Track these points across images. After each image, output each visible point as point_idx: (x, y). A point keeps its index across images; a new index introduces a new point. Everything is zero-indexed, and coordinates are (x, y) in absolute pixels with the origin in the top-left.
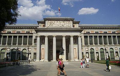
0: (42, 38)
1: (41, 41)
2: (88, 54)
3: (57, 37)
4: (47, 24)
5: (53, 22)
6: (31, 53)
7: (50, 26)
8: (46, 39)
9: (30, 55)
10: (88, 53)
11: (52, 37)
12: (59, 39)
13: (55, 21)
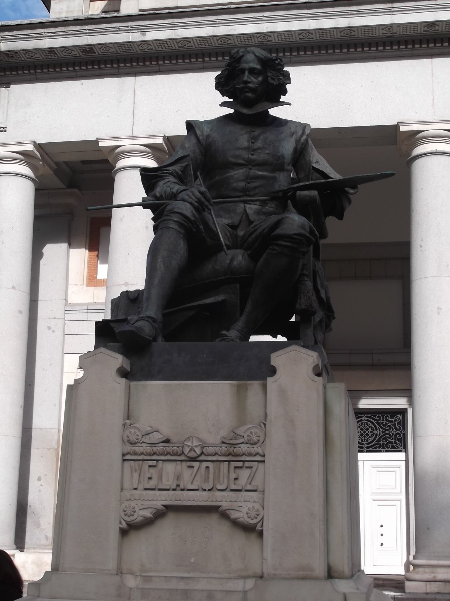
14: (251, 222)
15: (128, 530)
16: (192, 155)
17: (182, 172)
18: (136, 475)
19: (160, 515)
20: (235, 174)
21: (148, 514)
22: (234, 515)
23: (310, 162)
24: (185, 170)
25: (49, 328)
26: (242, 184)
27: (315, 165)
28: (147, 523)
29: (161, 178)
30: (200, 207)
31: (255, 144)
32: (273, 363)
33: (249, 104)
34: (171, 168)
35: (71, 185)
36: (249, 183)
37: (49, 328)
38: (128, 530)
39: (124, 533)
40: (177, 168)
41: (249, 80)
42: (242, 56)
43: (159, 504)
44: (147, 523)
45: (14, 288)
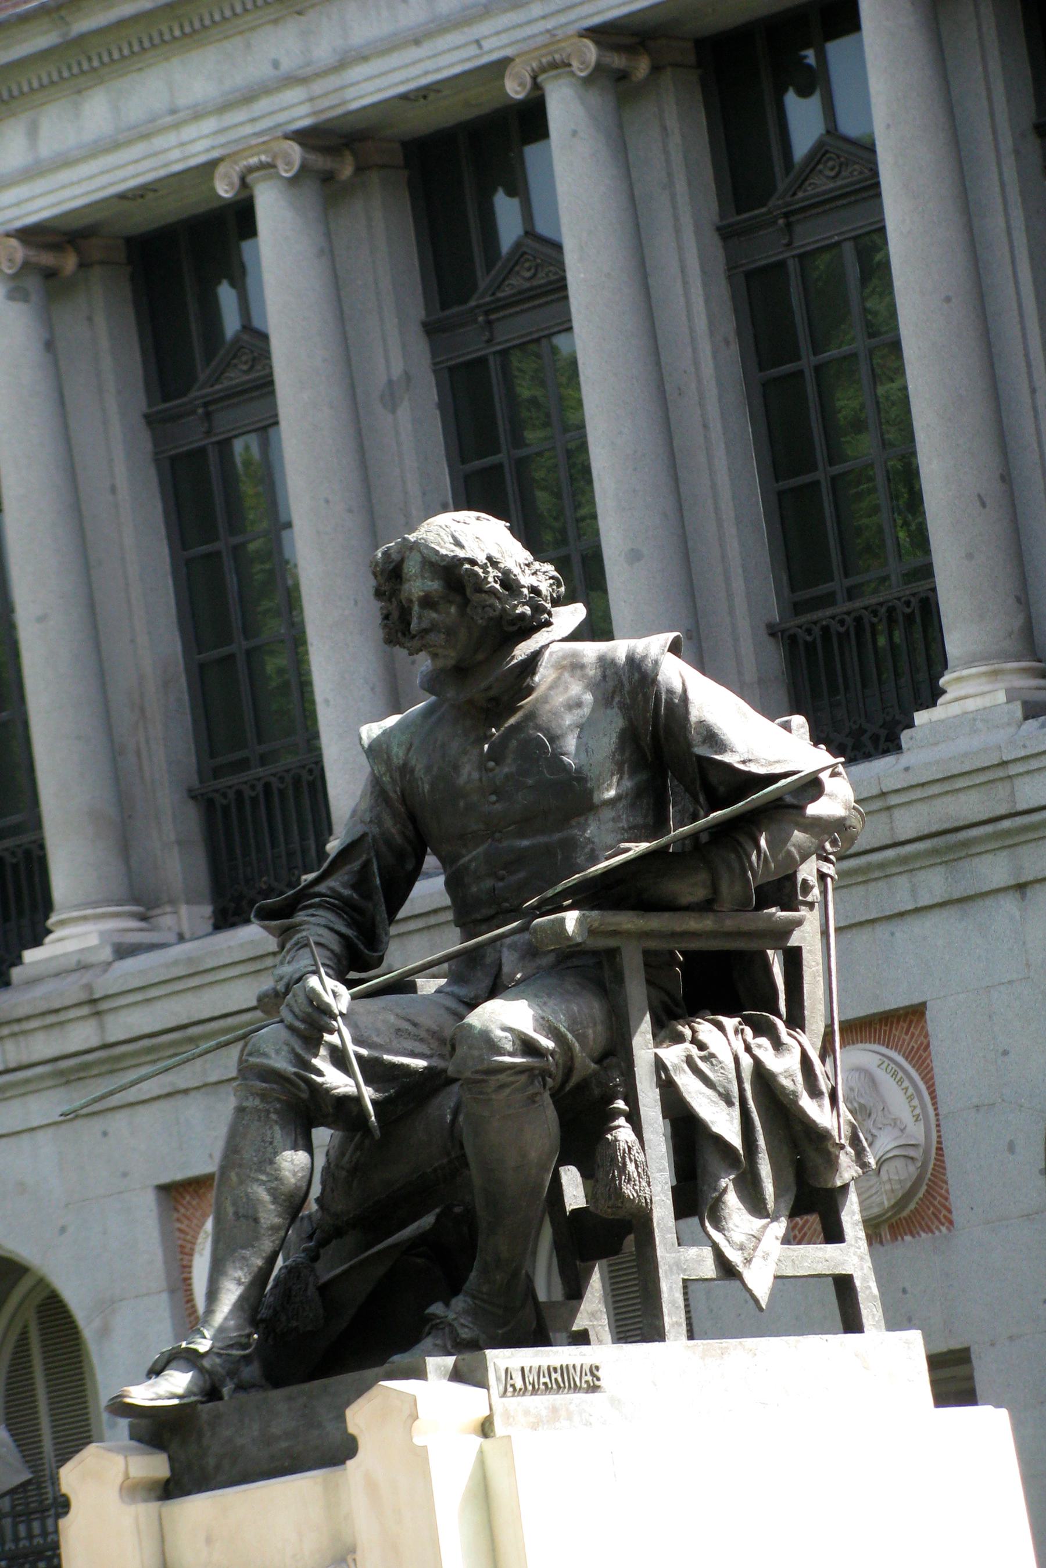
16: (375, 830)
17: (354, 887)
20: (470, 861)
23: (689, 746)
24: (361, 882)
26: (488, 883)
27: (701, 751)
31: (497, 770)
32: (352, 1429)
34: (322, 888)
36: (502, 879)
41: (425, 625)
42: (402, 561)
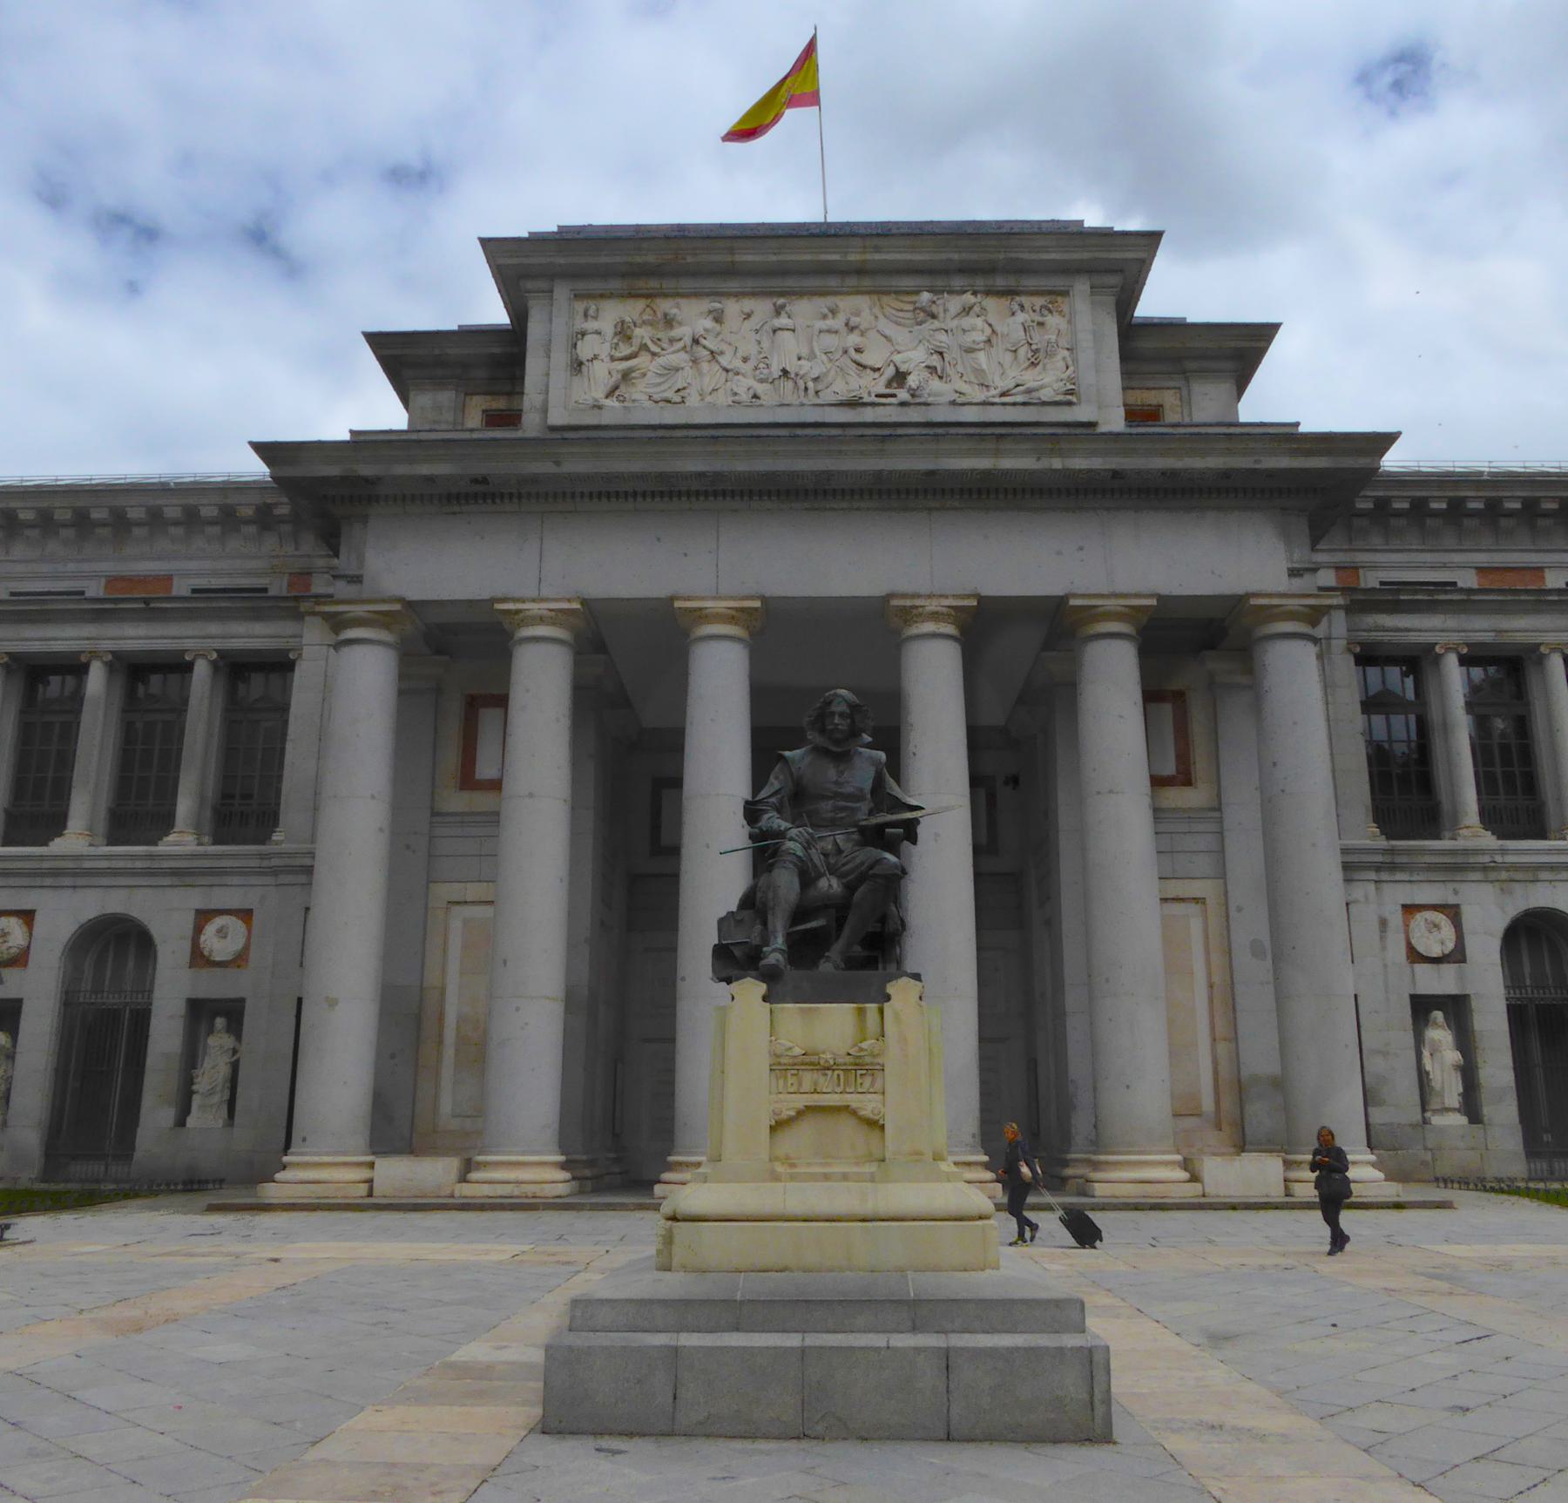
0: (455, 665)
1: (451, 758)
2: (1465, 1041)
3: (772, 627)
4: (560, 358)
5: (693, 316)
6: (233, 1012)
7: (613, 413)
8: (542, 686)
9: (218, 1043)
10: (1456, 1008)
11: (665, 633)
12: (825, 712)
13: (732, 308)
14: (839, 851)
15: (777, 1127)
18: (781, 1082)
19: (800, 1114)
21: (793, 1113)
22: (862, 1113)
24: (781, 801)
25: (408, 847)
26: (830, 815)
28: (790, 1121)
29: (766, 812)
30: (807, 846)
33: (837, 742)
35: (439, 652)
37: (408, 847)
38: (777, 1127)
39: (772, 1129)
40: (773, 800)
43: (800, 1105)
44: (790, 1121)
45: (373, 797)
